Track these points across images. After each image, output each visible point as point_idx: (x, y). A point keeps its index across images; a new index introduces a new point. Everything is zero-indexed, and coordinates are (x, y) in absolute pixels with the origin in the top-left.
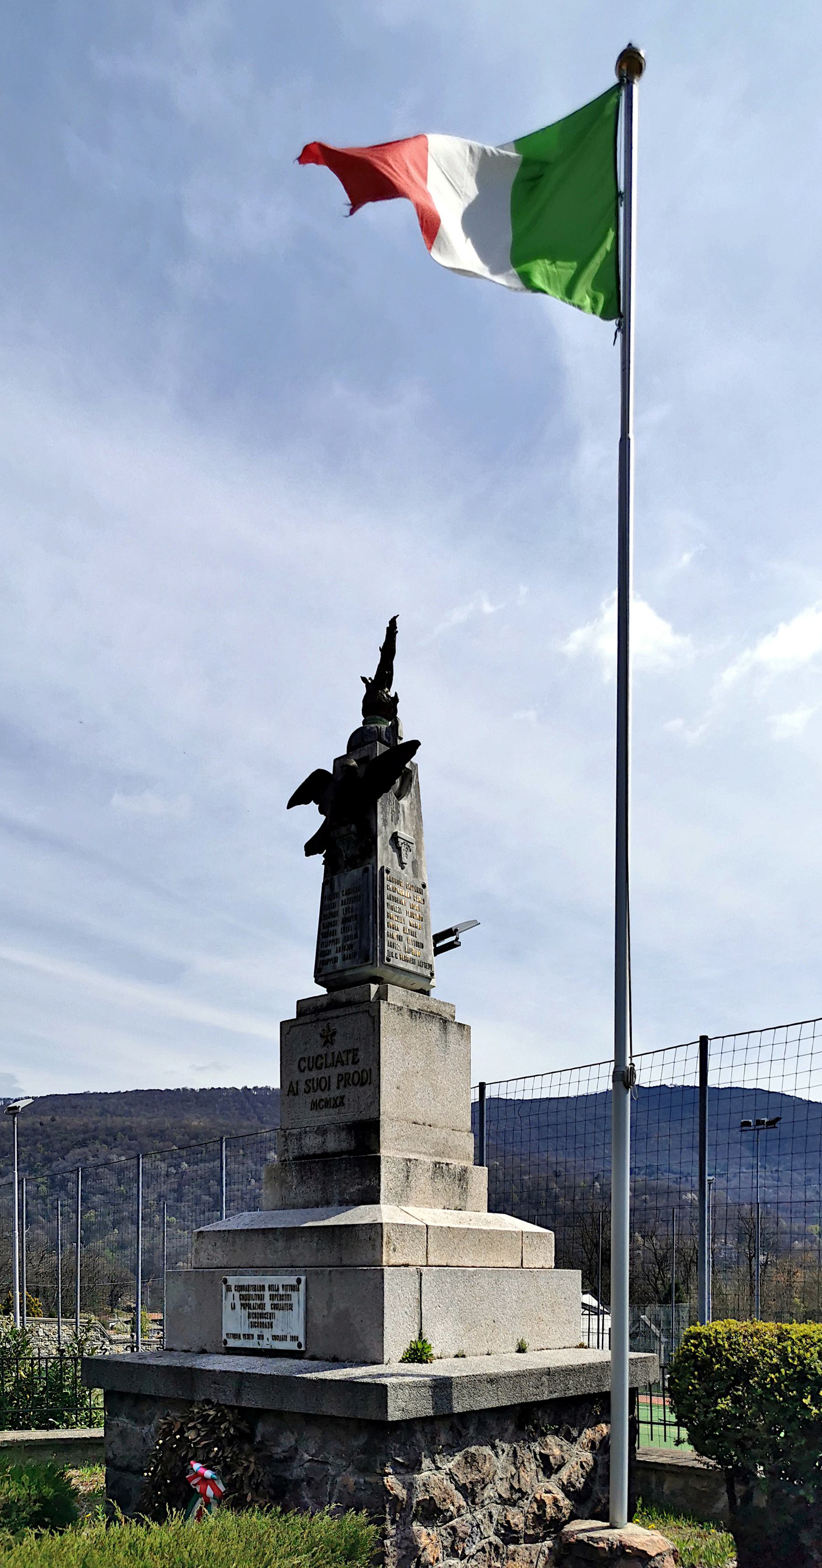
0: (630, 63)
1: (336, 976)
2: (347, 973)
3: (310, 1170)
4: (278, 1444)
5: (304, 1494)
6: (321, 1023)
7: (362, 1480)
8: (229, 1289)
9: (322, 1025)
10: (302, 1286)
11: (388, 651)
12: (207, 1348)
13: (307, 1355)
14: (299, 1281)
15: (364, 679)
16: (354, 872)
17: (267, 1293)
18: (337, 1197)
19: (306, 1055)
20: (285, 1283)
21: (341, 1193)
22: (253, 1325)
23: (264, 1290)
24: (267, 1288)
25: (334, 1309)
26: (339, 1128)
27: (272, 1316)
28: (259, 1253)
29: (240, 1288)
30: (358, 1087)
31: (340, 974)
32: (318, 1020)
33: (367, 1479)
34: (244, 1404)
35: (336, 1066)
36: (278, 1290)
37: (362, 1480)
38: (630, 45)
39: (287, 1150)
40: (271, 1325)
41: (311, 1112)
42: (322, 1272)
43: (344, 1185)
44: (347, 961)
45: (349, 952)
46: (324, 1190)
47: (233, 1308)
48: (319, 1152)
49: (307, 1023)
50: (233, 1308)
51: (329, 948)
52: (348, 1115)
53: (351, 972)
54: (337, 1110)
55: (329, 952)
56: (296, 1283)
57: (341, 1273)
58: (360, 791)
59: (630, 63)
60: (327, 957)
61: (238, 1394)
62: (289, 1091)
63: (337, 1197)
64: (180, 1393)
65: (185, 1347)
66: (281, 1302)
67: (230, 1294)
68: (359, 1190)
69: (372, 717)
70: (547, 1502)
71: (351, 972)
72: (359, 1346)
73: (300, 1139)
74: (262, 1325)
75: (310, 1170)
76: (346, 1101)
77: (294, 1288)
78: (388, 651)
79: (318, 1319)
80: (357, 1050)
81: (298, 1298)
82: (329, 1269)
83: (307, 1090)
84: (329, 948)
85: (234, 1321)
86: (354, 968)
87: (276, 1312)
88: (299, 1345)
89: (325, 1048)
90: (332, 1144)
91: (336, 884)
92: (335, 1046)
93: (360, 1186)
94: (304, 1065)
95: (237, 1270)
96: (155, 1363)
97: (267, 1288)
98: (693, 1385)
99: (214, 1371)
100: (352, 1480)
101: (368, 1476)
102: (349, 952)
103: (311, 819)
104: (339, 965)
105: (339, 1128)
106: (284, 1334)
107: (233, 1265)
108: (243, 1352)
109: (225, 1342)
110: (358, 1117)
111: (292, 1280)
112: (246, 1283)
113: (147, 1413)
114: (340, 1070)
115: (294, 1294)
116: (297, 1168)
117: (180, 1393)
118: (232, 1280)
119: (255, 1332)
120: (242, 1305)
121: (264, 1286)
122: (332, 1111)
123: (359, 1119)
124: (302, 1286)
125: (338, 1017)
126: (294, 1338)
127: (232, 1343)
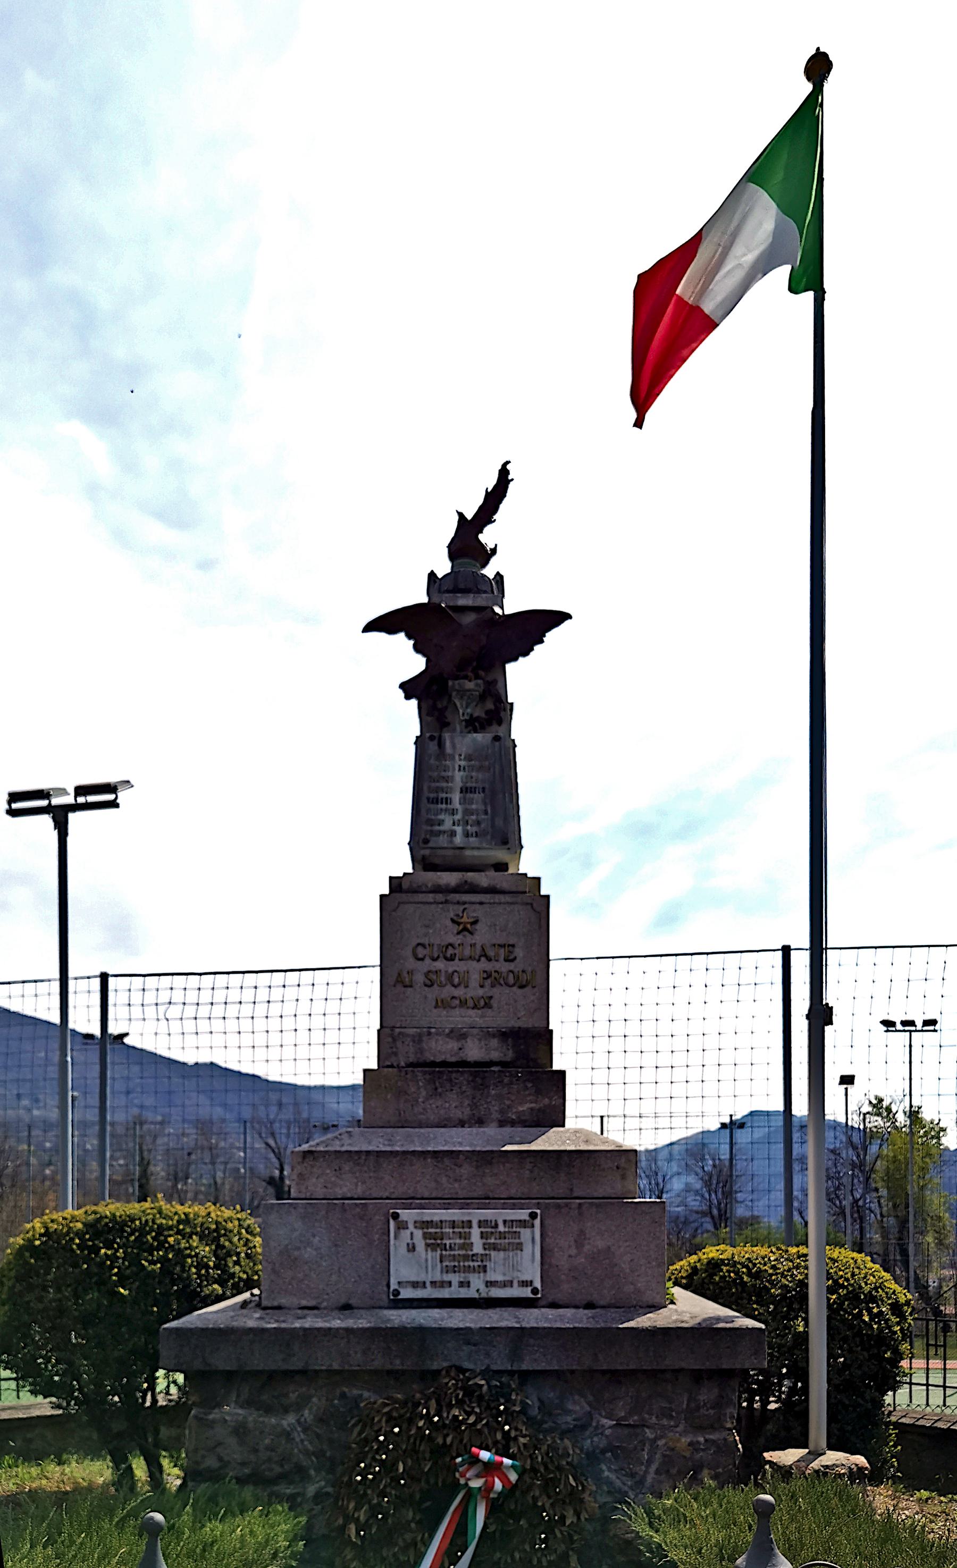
0: (819, 67)
1: (450, 853)
2: (468, 853)
3: (450, 1080)
4: (568, 1412)
5: (604, 1468)
6: (451, 907)
7: (701, 1439)
8: (402, 1226)
9: (452, 911)
10: (537, 1222)
11: (494, 499)
12: (353, 1302)
13: (543, 1303)
14: (533, 1216)
15: (461, 515)
16: (479, 737)
17: (467, 1230)
18: (496, 1115)
19: (426, 941)
20: (508, 1218)
21: (501, 1111)
22: (447, 1270)
23: (470, 1227)
24: (475, 1224)
25: (587, 1247)
26: (487, 1034)
27: (484, 1257)
28: (424, 1179)
29: (423, 1225)
30: (515, 989)
31: (457, 852)
32: (446, 902)
33: (707, 1437)
34: (524, 1367)
35: (479, 961)
36: (496, 1226)
37: (701, 1439)
38: (818, 49)
39: (396, 1054)
40: (485, 1269)
41: (435, 1011)
42: (567, 1205)
43: (507, 1102)
44: (472, 839)
45: (475, 829)
46: (474, 1106)
47: (412, 1248)
48: (453, 1059)
49: (431, 903)
50: (412, 1248)
51: (441, 817)
52: (499, 1019)
53: (476, 853)
54: (480, 1012)
55: (441, 823)
56: (527, 1218)
57: (598, 1206)
58: (465, 642)
59: (819, 67)
60: (437, 828)
61: (515, 1355)
62: (397, 981)
63: (496, 1115)
64: (398, 1362)
65: (312, 1303)
66: (502, 1241)
67: (405, 1234)
68: (532, 1109)
69: (473, 562)
70: (689, 1440)
71: (476, 853)
72: (629, 1288)
73: (420, 1041)
74: (468, 1269)
75: (450, 1080)
76: (494, 1003)
77: (523, 1224)
78: (494, 499)
79: (561, 1260)
80: (513, 946)
81: (531, 1238)
82: (578, 1201)
83: (428, 982)
84: (441, 817)
85: (410, 1266)
86: (478, 848)
87: (493, 1253)
88: (535, 1291)
89: (460, 936)
90: (474, 1051)
91: (448, 744)
92: (477, 937)
93: (533, 1105)
94: (421, 952)
95: (410, 1201)
96: (343, 1325)
97: (475, 1224)
98: (756, 1309)
99: (470, 1329)
100: (685, 1440)
101: (710, 1433)
102: (475, 829)
103: (404, 658)
104: (459, 840)
105: (487, 1034)
106: (507, 1278)
107: (374, 1195)
108: (424, 1304)
109: (396, 1293)
110: (514, 1023)
111: (523, 1214)
112: (436, 1218)
113: (293, 1396)
114: (484, 965)
115: (525, 1234)
116: (428, 1077)
117: (398, 1362)
118: (405, 1214)
119: (455, 1278)
120: (427, 1245)
121: (470, 1222)
122: (471, 1012)
123: (517, 1025)
124: (537, 1222)
125: (481, 903)
126: (524, 1284)
127: (406, 1293)
